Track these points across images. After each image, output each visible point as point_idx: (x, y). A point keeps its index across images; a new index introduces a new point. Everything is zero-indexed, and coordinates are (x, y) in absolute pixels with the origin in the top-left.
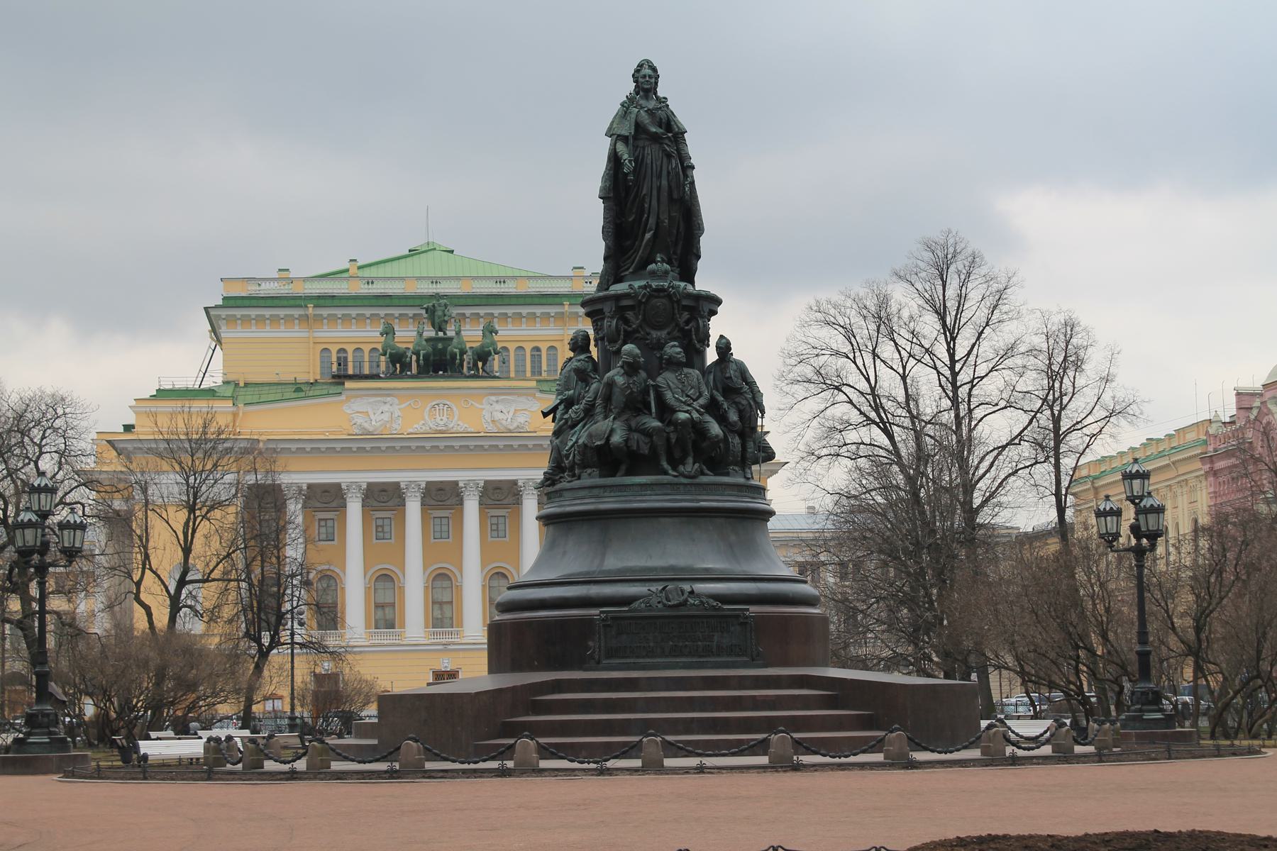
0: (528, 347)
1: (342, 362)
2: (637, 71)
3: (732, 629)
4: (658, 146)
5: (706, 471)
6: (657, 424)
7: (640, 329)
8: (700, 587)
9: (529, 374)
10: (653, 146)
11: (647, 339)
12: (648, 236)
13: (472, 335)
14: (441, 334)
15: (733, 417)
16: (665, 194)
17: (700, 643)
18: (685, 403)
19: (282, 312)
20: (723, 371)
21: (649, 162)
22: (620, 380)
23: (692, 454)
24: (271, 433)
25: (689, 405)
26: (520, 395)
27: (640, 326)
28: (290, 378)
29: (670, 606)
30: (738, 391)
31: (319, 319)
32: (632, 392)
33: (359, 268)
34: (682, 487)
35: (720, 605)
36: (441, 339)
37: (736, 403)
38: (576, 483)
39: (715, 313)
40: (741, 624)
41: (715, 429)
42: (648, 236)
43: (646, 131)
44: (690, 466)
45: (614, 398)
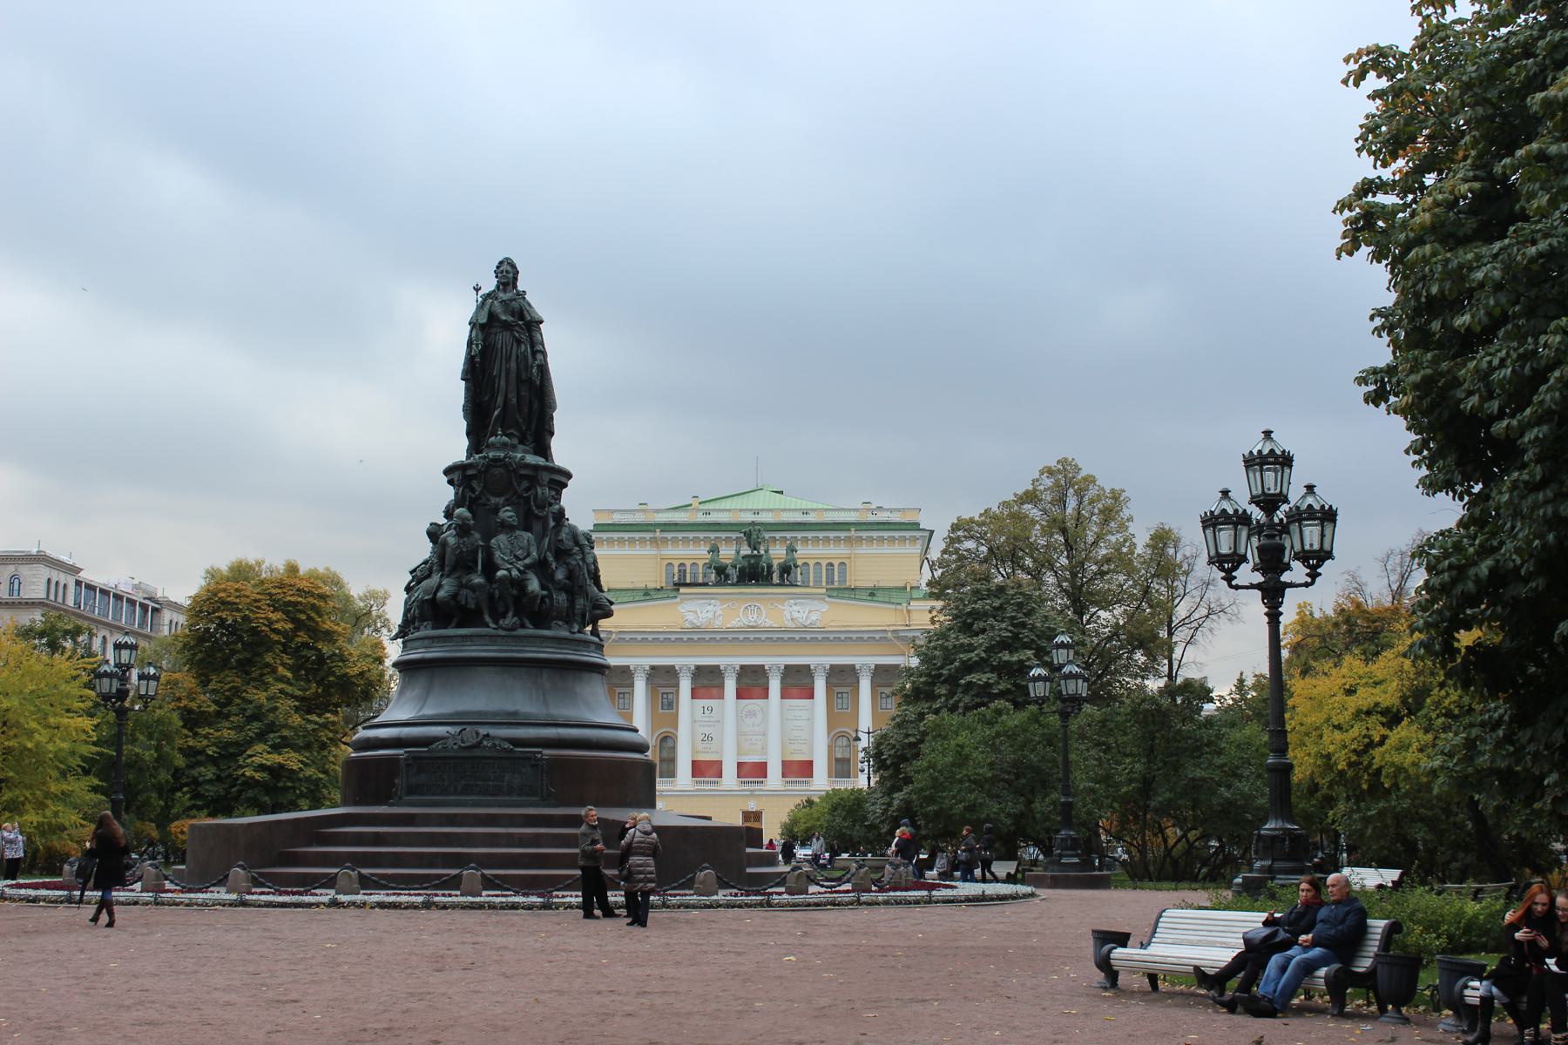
0: (824, 563)
1: (682, 572)
2: (498, 267)
3: (524, 770)
4: (509, 333)
5: (528, 624)
6: (478, 580)
8: (494, 731)
9: (824, 584)
12: (496, 413)
13: (777, 554)
14: (755, 552)
15: (560, 575)
16: (513, 376)
18: (507, 561)
19: (637, 535)
20: (557, 533)
21: (499, 346)
22: (452, 541)
23: (512, 608)
24: (624, 627)
25: (511, 564)
26: (813, 599)
27: (481, 493)
28: (642, 586)
30: (568, 553)
31: (664, 540)
32: (461, 552)
33: (700, 503)
34: (499, 639)
36: (754, 556)
37: (565, 563)
38: (417, 634)
39: (565, 486)
40: (533, 766)
41: (534, 585)
42: (496, 413)
43: (499, 320)
44: (510, 620)
45: (447, 557)
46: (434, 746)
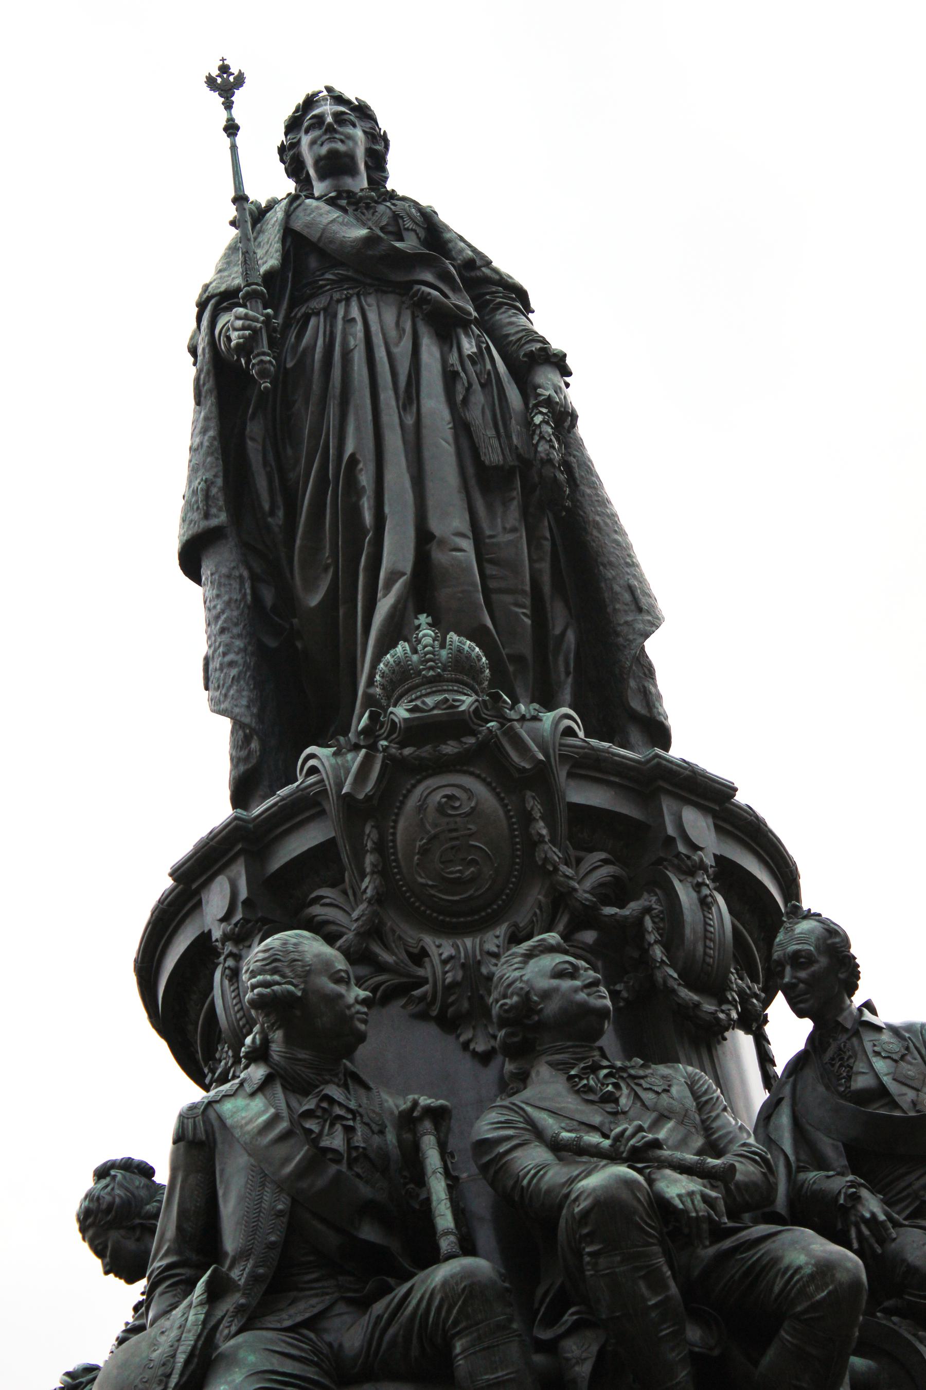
7: (377, 949)
10: (371, 300)
11: (423, 981)
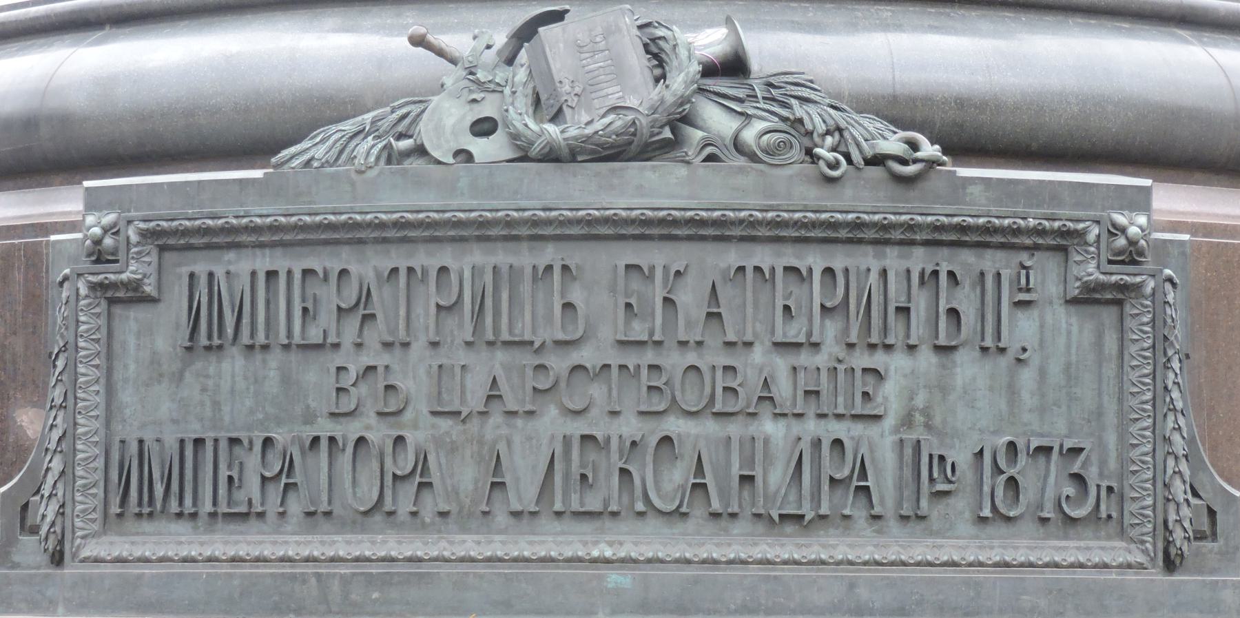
17: (770, 427)
29: (552, 156)
35: (929, 150)
46: (317, 147)
